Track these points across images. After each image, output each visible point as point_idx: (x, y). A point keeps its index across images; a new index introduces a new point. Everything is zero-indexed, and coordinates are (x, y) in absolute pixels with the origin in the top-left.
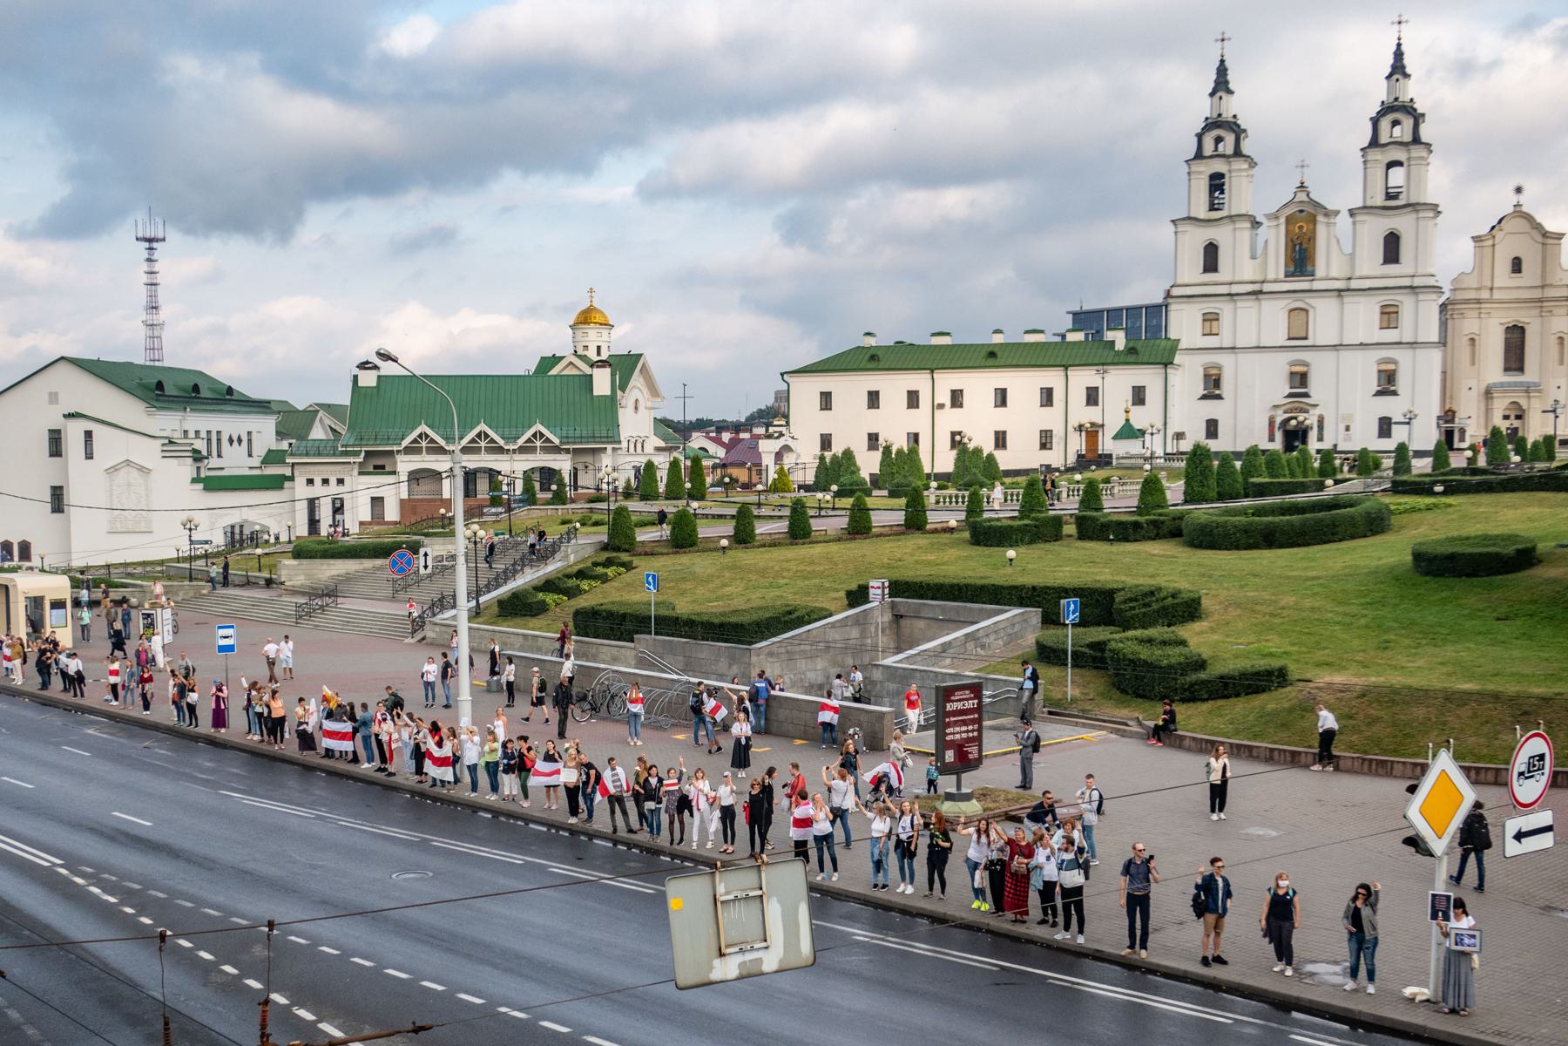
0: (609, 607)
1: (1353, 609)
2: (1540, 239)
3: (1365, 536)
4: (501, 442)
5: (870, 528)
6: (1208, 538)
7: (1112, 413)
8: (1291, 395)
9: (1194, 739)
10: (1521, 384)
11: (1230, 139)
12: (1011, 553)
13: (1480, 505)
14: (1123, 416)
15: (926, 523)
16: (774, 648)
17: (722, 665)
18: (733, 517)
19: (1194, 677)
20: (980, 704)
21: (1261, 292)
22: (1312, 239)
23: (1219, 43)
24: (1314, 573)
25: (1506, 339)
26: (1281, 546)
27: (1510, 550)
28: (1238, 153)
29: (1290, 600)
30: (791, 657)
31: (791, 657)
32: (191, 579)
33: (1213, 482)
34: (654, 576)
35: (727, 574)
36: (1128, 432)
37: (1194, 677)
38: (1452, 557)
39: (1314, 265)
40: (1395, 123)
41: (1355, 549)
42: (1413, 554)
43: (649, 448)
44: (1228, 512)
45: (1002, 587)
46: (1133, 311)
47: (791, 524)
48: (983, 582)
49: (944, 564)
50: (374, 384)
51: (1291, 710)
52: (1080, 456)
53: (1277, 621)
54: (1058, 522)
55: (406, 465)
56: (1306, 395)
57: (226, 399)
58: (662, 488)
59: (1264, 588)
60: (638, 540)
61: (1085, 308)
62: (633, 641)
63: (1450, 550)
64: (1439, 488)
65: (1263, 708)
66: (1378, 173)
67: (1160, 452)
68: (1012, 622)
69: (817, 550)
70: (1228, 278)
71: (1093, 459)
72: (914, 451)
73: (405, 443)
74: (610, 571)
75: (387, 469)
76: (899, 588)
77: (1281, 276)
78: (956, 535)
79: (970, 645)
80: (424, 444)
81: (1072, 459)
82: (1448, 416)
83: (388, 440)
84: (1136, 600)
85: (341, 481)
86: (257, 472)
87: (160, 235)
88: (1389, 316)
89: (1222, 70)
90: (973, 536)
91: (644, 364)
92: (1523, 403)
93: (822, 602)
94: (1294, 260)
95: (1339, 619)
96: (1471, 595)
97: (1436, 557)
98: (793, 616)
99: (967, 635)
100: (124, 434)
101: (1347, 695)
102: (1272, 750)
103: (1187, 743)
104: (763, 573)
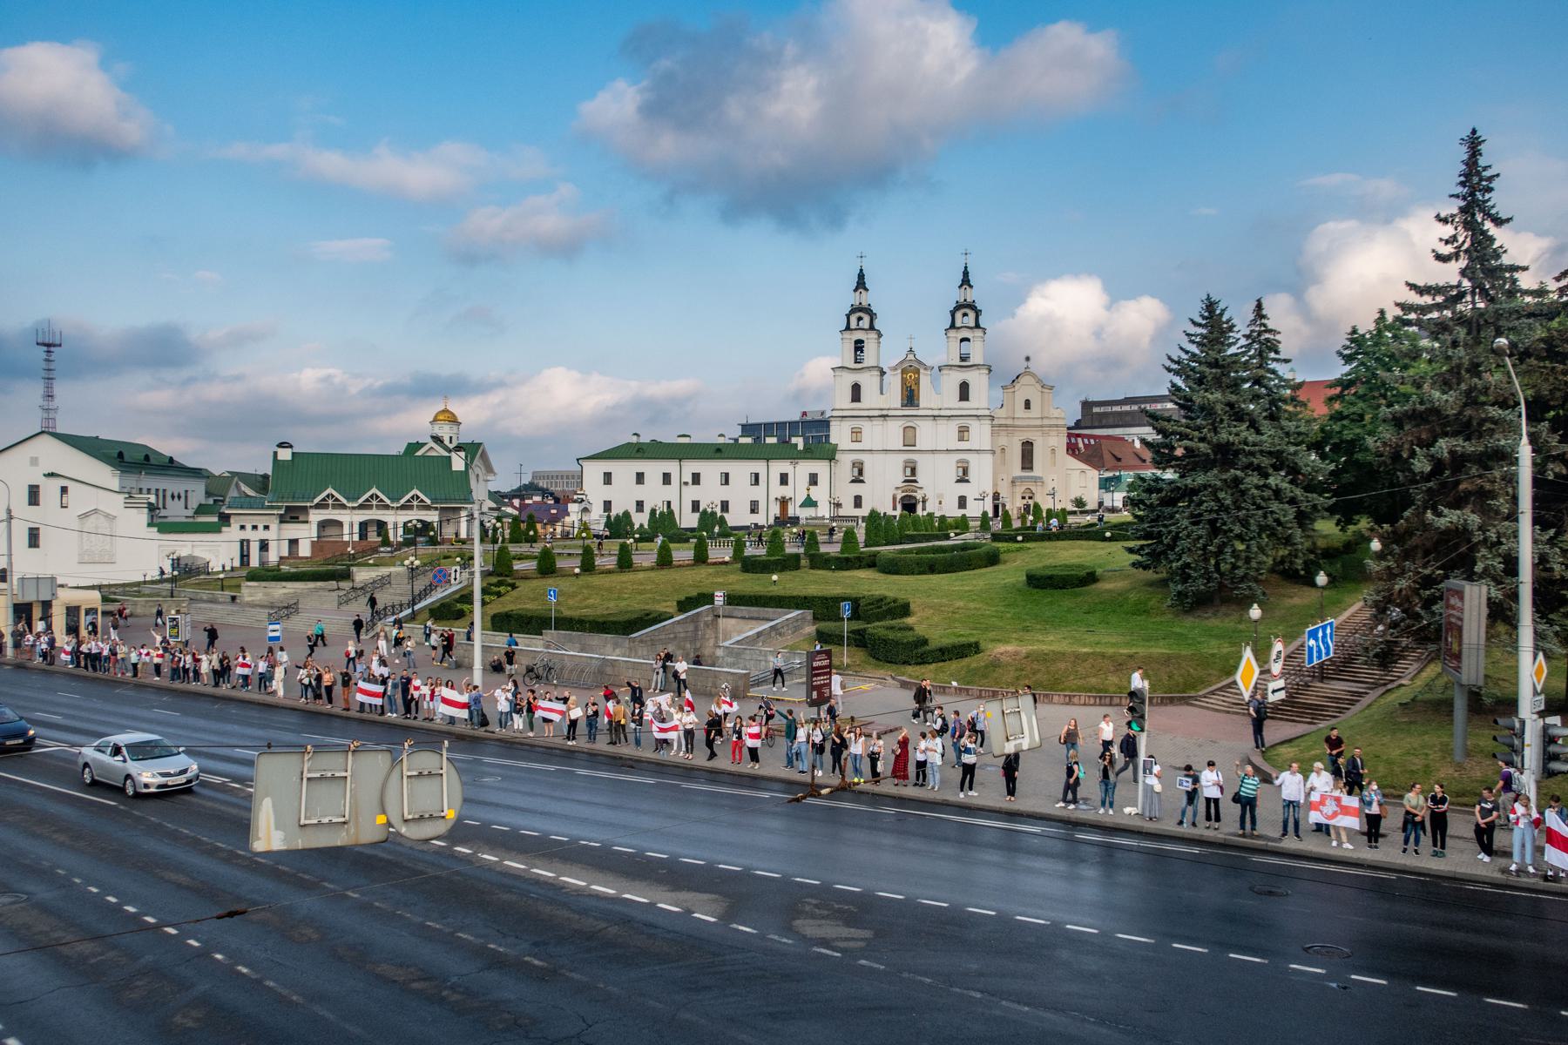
2: (1040, 388)
3: (986, 567)
4: (388, 502)
5: (672, 562)
6: (892, 567)
7: (798, 489)
8: (905, 481)
10: (1032, 477)
11: (866, 319)
12: (775, 577)
13: (1046, 549)
14: (806, 493)
15: (707, 558)
16: (644, 638)
17: (609, 648)
18: (536, 558)
19: (921, 650)
21: (887, 416)
22: (917, 383)
23: (859, 259)
24: (970, 588)
25: (1023, 450)
26: (939, 573)
27: (1083, 573)
28: (872, 328)
29: (961, 604)
30: (653, 643)
31: (653, 643)
32: (172, 596)
33: (882, 534)
34: (554, 591)
35: (585, 591)
36: (809, 503)
37: (921, 650)
38: (1051, 577)
39: (918, 400)
40: (965, 315)
41: (984, 574)
42: (1027, 576)
43: (485, 509)
44: (902, 551)
45: (785, 597)
46: (781, 425)
48: (771, 594)
49: (730, 584)
50: (290, 458)
51: (986, 667)
52: (776, 518)
53: (957, 616)
54: (797, 557)
55: (316, 516)
56: (915, 481)
57: (170, 467)
60: (515, 568)
61: (750, 422)
63: (1049, 573)
64: (1020, 538)
65: (968, 666)
67: (827, 516)
68: (796, 619)
69: (641, 575)
71: (784, 520)
72: (671, 513)
73: (316, 501)
74: (502, 589)
75: (301, 519)
76: (732, 600)
77: (899, 406)
78: (729, 567)
79: (773, 634)
80: (330, 502)
81: (771, 521)
82: (996, 496)
83: (303, 499)
84: (873, 604)
85: (266, 527)
86: (191, 520)
87: (57, 342)
88: (963, 432)
89: (861, 276)
90: (743, 567)
92: (1033, 488)
94: (908, 397)
97: (1042, 577)
98: (651, 617)
99: (771, 627)
101: (1017, 657)
102: (981, 691)
104: (610, 590)
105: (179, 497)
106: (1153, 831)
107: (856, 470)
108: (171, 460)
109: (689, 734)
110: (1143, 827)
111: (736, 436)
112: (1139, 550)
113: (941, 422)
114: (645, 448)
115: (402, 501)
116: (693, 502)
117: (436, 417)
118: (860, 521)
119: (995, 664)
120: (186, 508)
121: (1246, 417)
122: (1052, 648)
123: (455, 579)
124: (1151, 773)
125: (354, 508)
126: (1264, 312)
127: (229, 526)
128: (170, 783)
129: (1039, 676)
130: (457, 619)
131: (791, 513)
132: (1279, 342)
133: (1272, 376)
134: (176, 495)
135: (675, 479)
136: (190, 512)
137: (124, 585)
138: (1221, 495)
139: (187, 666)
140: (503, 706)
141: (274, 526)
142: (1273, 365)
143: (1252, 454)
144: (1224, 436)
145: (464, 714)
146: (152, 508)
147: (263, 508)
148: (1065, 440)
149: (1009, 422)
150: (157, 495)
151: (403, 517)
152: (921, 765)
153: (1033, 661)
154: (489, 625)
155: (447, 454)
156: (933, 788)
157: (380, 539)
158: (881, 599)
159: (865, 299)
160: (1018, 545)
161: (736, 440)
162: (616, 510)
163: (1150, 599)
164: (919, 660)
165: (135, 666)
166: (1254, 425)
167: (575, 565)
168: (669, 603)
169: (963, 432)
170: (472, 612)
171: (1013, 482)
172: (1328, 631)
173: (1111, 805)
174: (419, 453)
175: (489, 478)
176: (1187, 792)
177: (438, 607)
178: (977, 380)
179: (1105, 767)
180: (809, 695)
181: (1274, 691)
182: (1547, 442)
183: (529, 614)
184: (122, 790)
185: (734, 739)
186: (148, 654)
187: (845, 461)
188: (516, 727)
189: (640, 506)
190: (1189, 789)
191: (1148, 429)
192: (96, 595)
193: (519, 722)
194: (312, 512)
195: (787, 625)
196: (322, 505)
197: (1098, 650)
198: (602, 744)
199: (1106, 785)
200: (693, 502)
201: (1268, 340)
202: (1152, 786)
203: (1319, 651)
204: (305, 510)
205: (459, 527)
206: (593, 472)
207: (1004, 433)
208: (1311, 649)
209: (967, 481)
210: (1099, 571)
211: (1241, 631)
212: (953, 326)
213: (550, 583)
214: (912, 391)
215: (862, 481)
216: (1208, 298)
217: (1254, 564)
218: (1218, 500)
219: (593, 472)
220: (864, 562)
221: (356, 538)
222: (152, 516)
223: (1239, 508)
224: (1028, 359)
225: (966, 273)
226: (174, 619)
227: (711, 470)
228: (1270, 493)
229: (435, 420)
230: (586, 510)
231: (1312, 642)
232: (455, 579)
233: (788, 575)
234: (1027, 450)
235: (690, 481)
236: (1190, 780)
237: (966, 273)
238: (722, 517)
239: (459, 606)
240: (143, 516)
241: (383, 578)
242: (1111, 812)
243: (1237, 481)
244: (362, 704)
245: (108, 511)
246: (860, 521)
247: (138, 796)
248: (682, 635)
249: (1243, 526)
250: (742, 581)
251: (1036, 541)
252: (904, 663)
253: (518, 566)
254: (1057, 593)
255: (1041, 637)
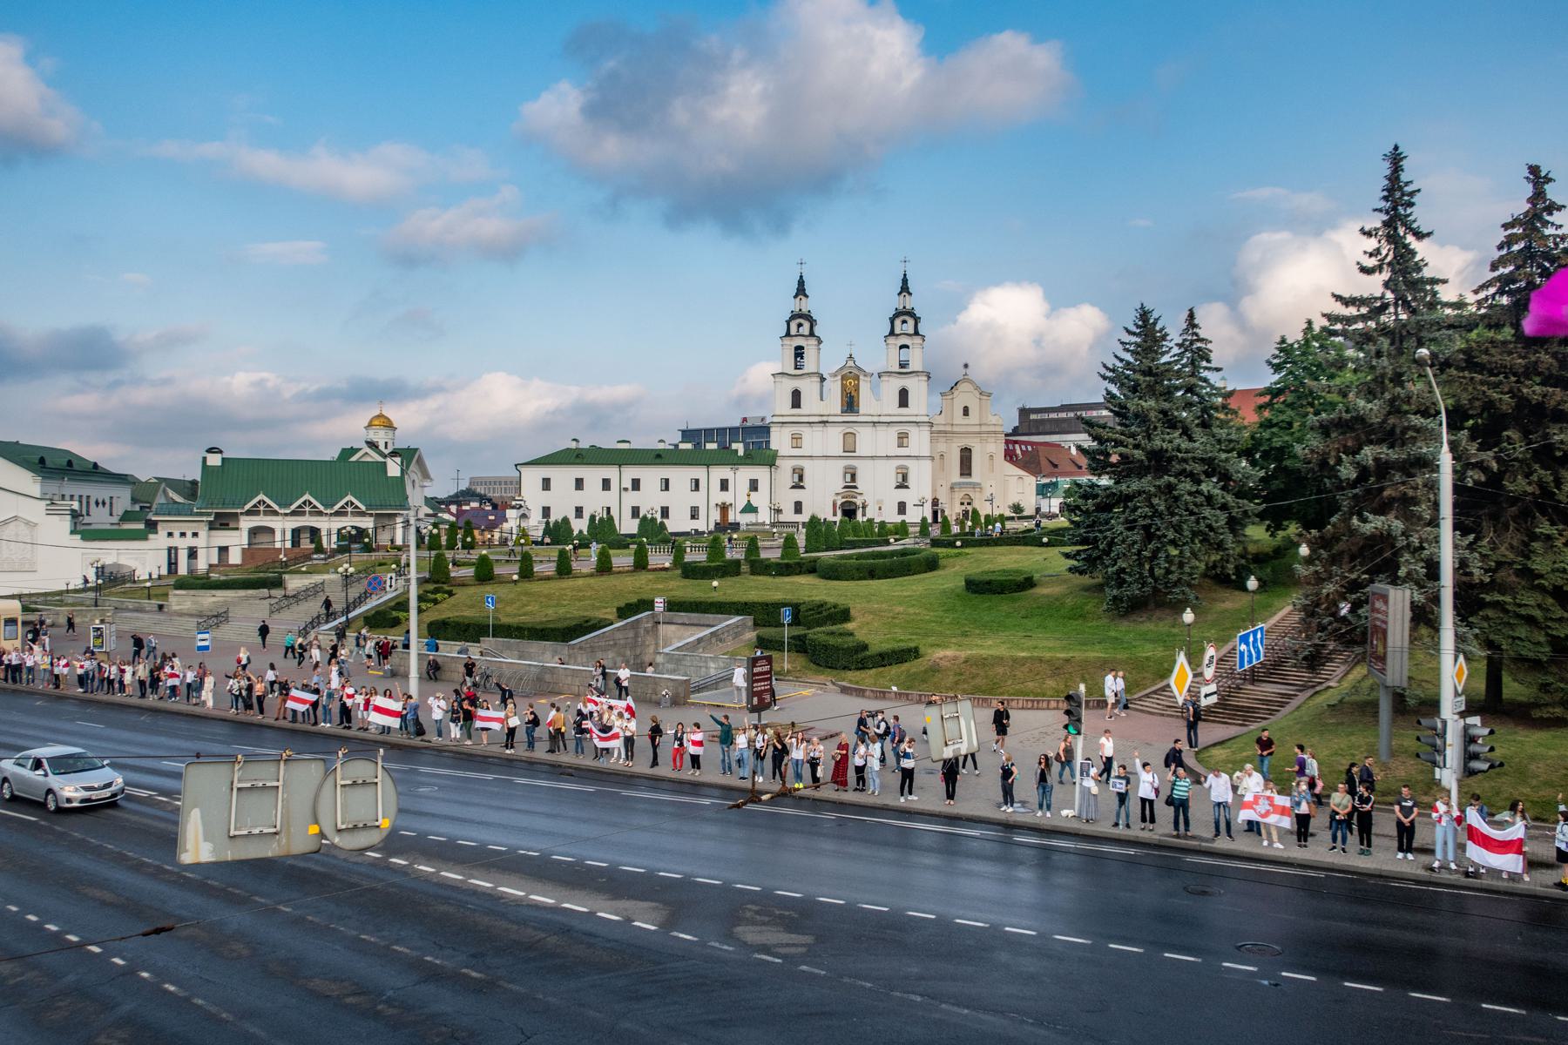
0: (457, 619)
1: (941, 614)
4: (321, 508)
6: (832, 573)
7: (738, 495)
8: (845, 487)
9: (872, 691)
10: (970, 483)
11: (806, 325)
12: (715, 583)
13: (985, 554)
17: (548, 655)
18: (474, 564)
19: (860, 656)
20: (771, 668)
21: (827, 422)
22: (857, 389)
24: (908, 593)
26: (879, 579)
27: (1021, 578)
28: (812, 334)
29: (901, 609)
30: (593, 650)
31: (593, 650)
32: (96, 606)
35: (524, 598)
36: (750, 508)
37: (860, 656)
38: (989, 583)
40: (904, 322)
43: (421, 516)
44: (843, 557)
45: (726, 603)
46: (721, 431)
47: (558, 565)
49: (671, 590)
51: (926, 672)
52: (717, 524)
54: (737, 563)
55: (246, 523)
56: (855, 487)
57: (94, 473)
58: (444, 543)
59: (882, 602)
60: (452, 575)
62: (479, 642)
63: (987, 578)
64: (958, 543)
65: (908, 671)
66: (894, 351)
68: (736, 625)
69: (580, 582)
70: (808, 413)
71: (724, 526)
72: (611, 519)
73: (247, 507)
74: (439, 596)
75: (231, 526)
76: (672, 606)
77: (839, 412)
78: (670, 573)
79: (714, 640)
80: (262, 508)
81: (712, 527)
82: (935, 502)
83: (234, 505)
85: (195, 535)
88: (902, 438)
89: (801, 283)
90: (683, 573)
91: (419, 456)
93: (600, 614)
95: (933, 619)
96: (1002, 606)
97: (981, 582)
98: (589, 624)
100: (15, 496)
101: (957, 662)
102: (920, 695)
103: (867, 693)
104: (549, 597)
105: (104, 503)
106: (1090, 833)
107: (796, 476)
108: (95, 465)
109: (629, 742)
110: (1079, 829)
111: (676, 442)
112: (1075, 555)
113: (880, 428)
114: (584, 453)
115: (336, 507)
116: (633, 507)
117: (371, 421)
118: (800, 526)
119: (935, 669)
120: (111, 515)
121: (1179, 425)
122: (990, 652)
123: (391, 586)
124: (1088, 775)
125: (286, 515)
126: (1196, 322)
127: (157, 533)
128: (94, 798)
129: (978, 681)
130: (392, 627)
131: (731, 519)
132: (1211, 351)
133: (1204, 384)
134: (100, 501)
135: (614, 485)
136: (115, 519)
137: (46, 594)
138: (1155, 501)
139: (112, 677)
140: (437, 715)
141: (203, 533)
142: (1205, 374)
143: (1185, 460)
144: (1157, 443)
145: (395, 723)
146: (75, 515)
147: (192, 514)
148: (1002, 447)
149: (948, 428)
150: (81, 502)
151: (338, 523)
152: (860, 770)
153: (971, 666)
154: (426, 632)
155: (382, 460)
156: (873, 793)
157: (313, 546)
158: (822, 605)
159: (806, 305)
160: (956, 551)
161: (677, 446)
162: (555, 516)
163: (1086, 604)
164: (860, 665)
165: (57, 677)
166: (1187, 433)
167: (512, 571)
168: (609, 610)
169: (902, 438)
170: (408, 620)
171: (952, 488)
172: (1259, 636)
173: (1049, 807)
174: (354, 459)
175: (425, 484)
176: (1119, 794)
177: (373, 615)
178: (917, 387)
179: (1043, 771)
180: (749, 700)
181: (1206, 696)
182: (1467, 450)
183: (466, 621)
184: (43, 805)
185: (676, 746)
186: (67, 665)
187: (785, 466)
188: (453, 736)
189: (579, 511)
190: (1123, 791)
191: (1084, 436)
192: (17, 604)
193: (455, 731)
194: (242, 518)
195: (728, 631)
196: (252, 512)
197: (1036, 654)
198: (541, 752)
199: (1044, 788)
200: (633, 507)
201: (1199, 349)
202: (1089, 789)
203: (1250, 656)
204: (235, 515)
205: (394, 533)
206: (532, 478)
207: (941, 439)
208: (1242, 654)
209: (907, 487)
210: (1036, 576)
211: (1174, 635)
212: (892, 333)
213: (488, 590)
214: (851, 397)
215: (802, 487)
216: (1142, 307)
217: (1187, 569)
218: (1152, 506)
219: (532, 478)
220: (804, 569)
221: (288, 545)
222: (75, 523)
223: (1172, 514)
224: (966, 366)
225: (905, 281)
226: (99, 629)
227: (650, 476)
228: (1203, 499)
229: (370, 425)
230: (524, 516)
231: (1243, 647)
232: (391, 586)
233: (729, 581)
234: (966, 457)
235: (630, 487)
236: (1124, 782)
237: (905, 281)
238: (662, 523)
239: (395, 614)
240: (66, 523)
241: (316, 585)
242: (1048, 815)
243: (1170, 487)
244: (294, 712)
245: (29, 518)
246: (800, 526)
247: (60, 811)
248: (622, 642)
249: (1176, 531)
250: (683, 587)
251: (974, 546)
252: (844, 668)
253: (455, 573)
254: (996, 598)
255: (979, 642)
